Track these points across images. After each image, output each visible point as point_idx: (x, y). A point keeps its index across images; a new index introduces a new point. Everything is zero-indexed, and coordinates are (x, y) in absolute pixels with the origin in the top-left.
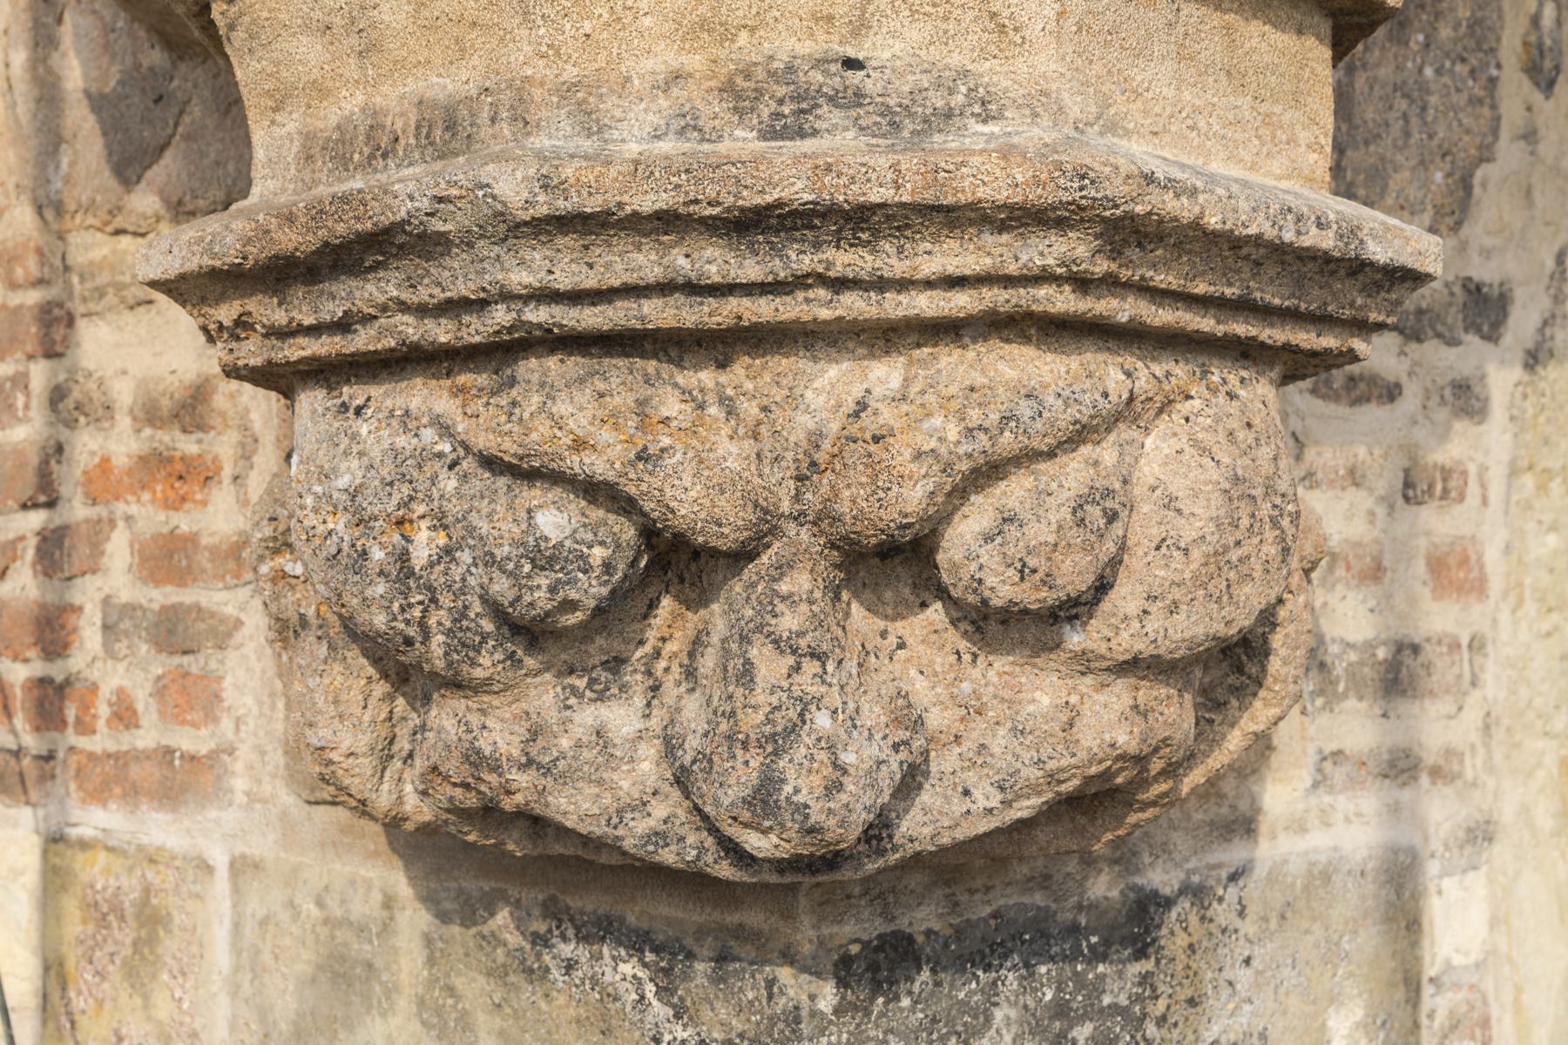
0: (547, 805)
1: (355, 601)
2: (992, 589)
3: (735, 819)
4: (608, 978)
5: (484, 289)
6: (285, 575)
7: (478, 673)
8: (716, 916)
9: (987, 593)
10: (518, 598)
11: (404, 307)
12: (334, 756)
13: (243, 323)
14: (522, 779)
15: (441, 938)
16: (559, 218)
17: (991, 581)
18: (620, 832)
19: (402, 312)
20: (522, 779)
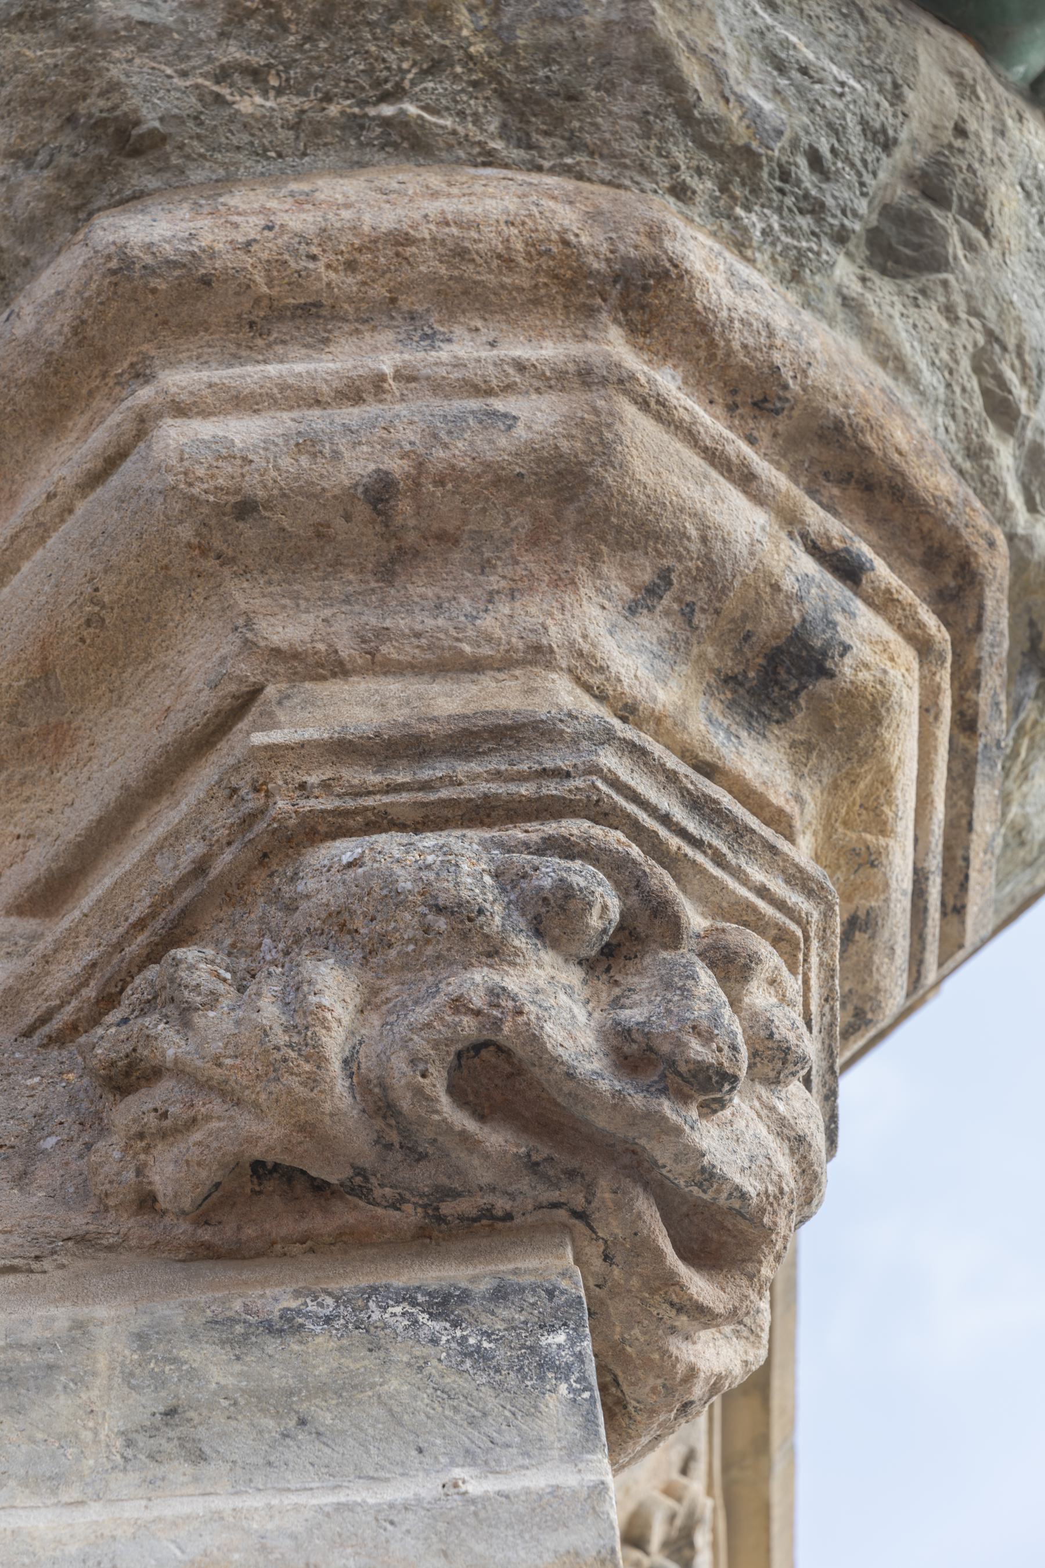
0: (542, 1028)
1: (446, 884)
2: (777, 1028)
3: (694, 1028)
4: (376, 1316)
5: (575, 766)
6: (218, 976)
7: (517, 943)
8: (492, 1268)
9: (775, 1030)
10: (586, 888)
11: (498, 776)
12: (328, 1015)
13: (326, 786)
14: (533, 1008)
15: (158, 1333)
16: (634, 745)
17: (777, 1023)
18: (576, 1063)
19: (487, 781)
20: (529, 1008)
